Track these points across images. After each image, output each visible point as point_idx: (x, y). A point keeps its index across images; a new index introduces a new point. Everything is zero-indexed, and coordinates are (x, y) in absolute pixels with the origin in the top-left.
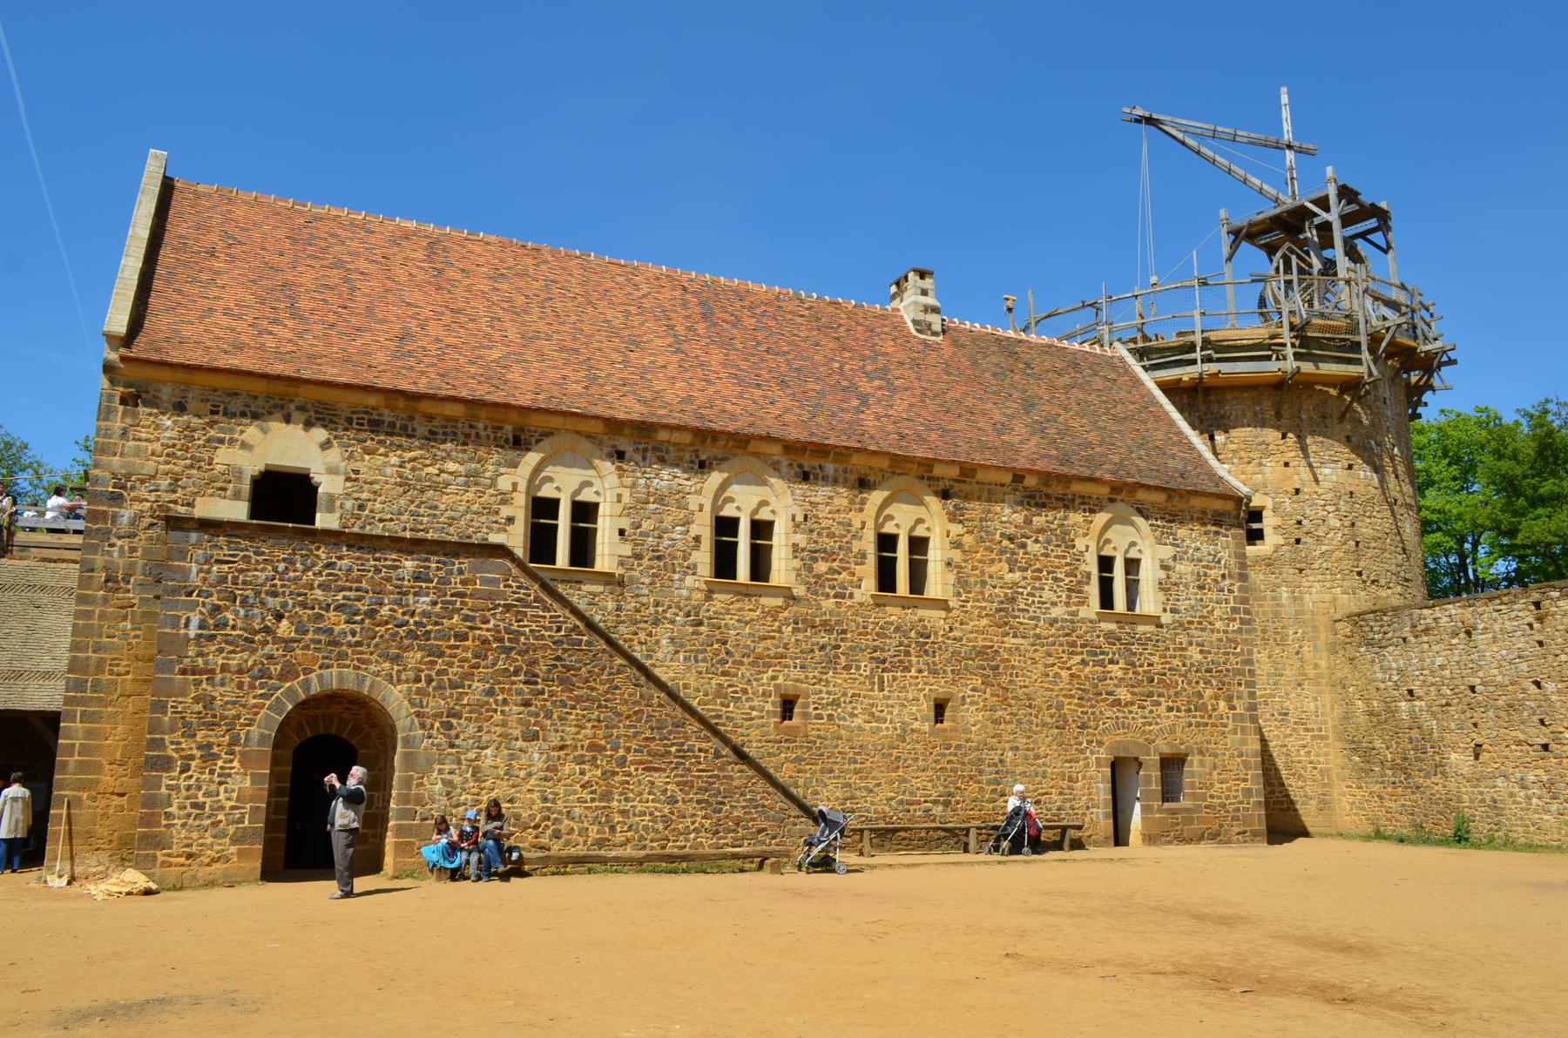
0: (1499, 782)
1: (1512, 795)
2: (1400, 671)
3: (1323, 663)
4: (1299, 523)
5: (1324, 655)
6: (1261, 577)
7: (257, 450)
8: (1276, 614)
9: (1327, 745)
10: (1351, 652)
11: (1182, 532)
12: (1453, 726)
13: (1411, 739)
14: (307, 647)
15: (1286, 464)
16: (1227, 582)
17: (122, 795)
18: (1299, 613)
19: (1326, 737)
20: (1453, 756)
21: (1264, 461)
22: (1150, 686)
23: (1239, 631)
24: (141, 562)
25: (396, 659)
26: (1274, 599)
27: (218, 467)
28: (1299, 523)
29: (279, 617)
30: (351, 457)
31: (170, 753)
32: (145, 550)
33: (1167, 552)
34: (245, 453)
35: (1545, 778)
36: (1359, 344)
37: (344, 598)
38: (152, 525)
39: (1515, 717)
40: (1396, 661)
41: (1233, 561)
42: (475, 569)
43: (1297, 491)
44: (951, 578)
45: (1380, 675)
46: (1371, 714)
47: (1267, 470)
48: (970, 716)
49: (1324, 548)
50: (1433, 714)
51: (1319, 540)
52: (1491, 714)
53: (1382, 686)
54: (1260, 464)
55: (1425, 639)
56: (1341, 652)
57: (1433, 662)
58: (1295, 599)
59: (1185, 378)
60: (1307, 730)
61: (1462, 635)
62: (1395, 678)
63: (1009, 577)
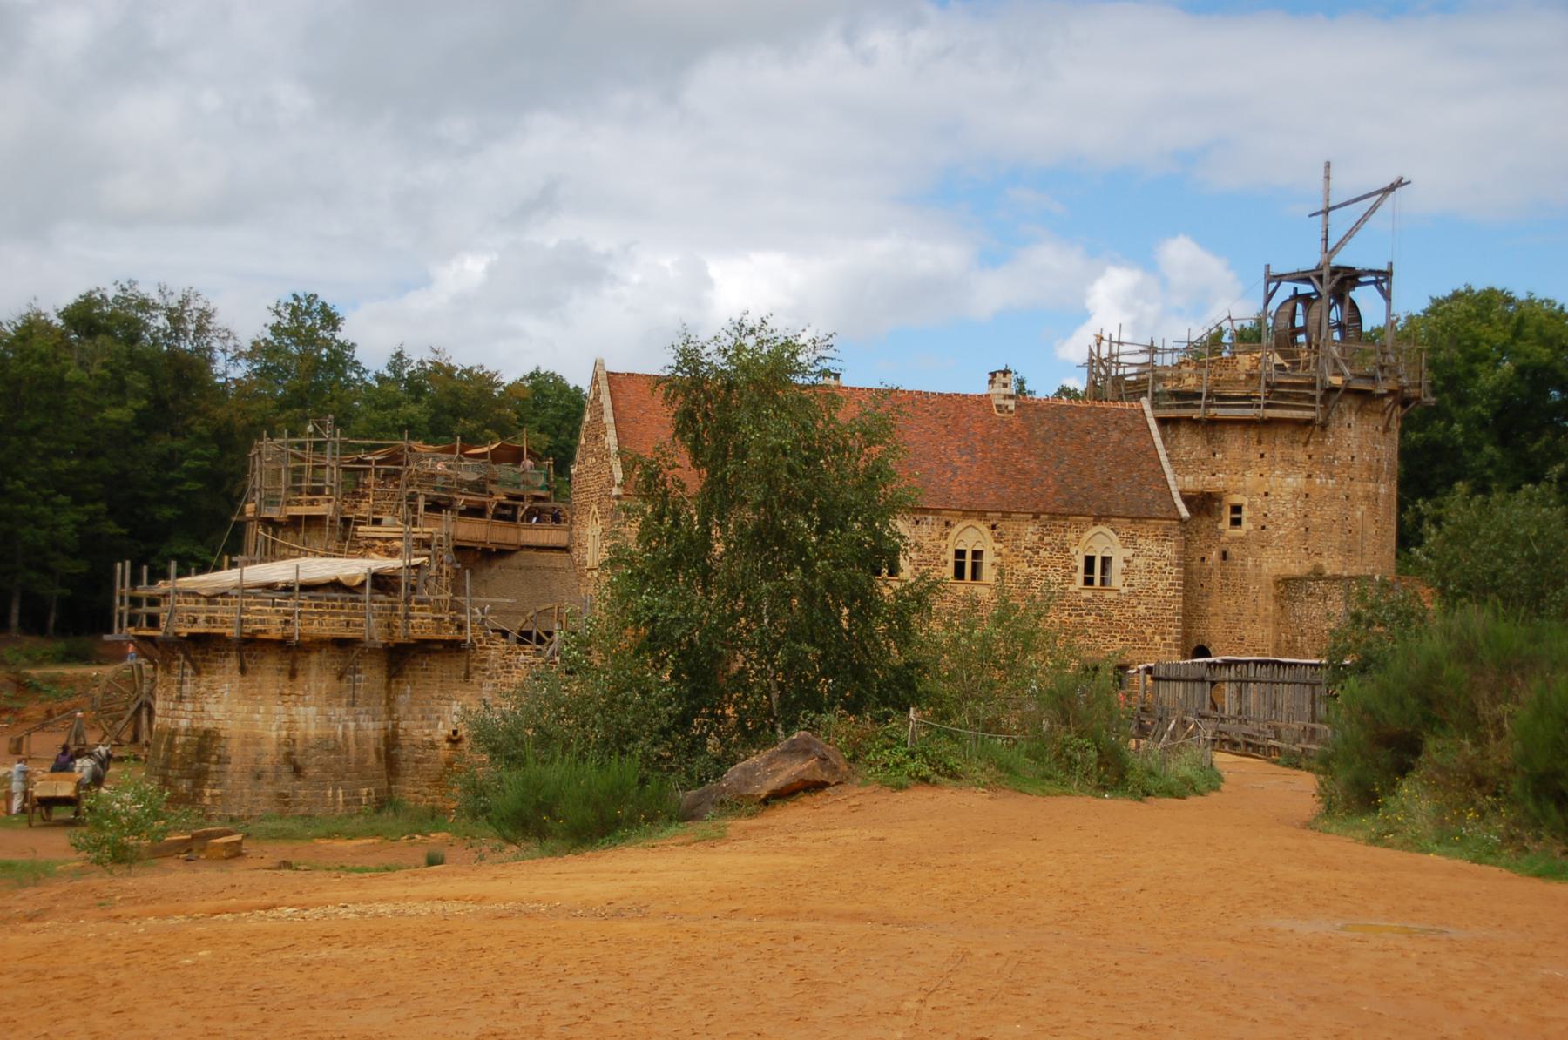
11: (1140, 541)
22: (1110, 627)
33: (1128, 553)
44: (995, 571)
51: (1278, 528)
63: (1028, 570)
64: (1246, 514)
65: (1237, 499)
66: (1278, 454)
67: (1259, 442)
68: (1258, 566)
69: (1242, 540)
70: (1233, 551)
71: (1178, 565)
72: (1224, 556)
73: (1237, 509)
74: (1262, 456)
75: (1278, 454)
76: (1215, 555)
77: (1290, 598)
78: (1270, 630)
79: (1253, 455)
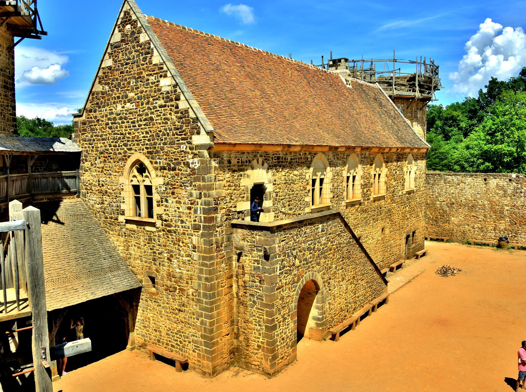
0: (466, 226)
1: (469, 230)
7: (251, 177)
13: (439, 213)
14: (302, 268)
17: (228, 335)
20: (453, 218)
24: (225, 236)
25: (318, 264)
27: (242, 188)
29: (295, 258)
30: (274, 174)
31: (276, 322)
32: (225, 230)
34: (247, 179)
35: (480, 226)
37: (309, 245)
38: (227, 219)
39: (474, 210)
42: (333, 223)
48: (387, 231)
52: (467, 208)
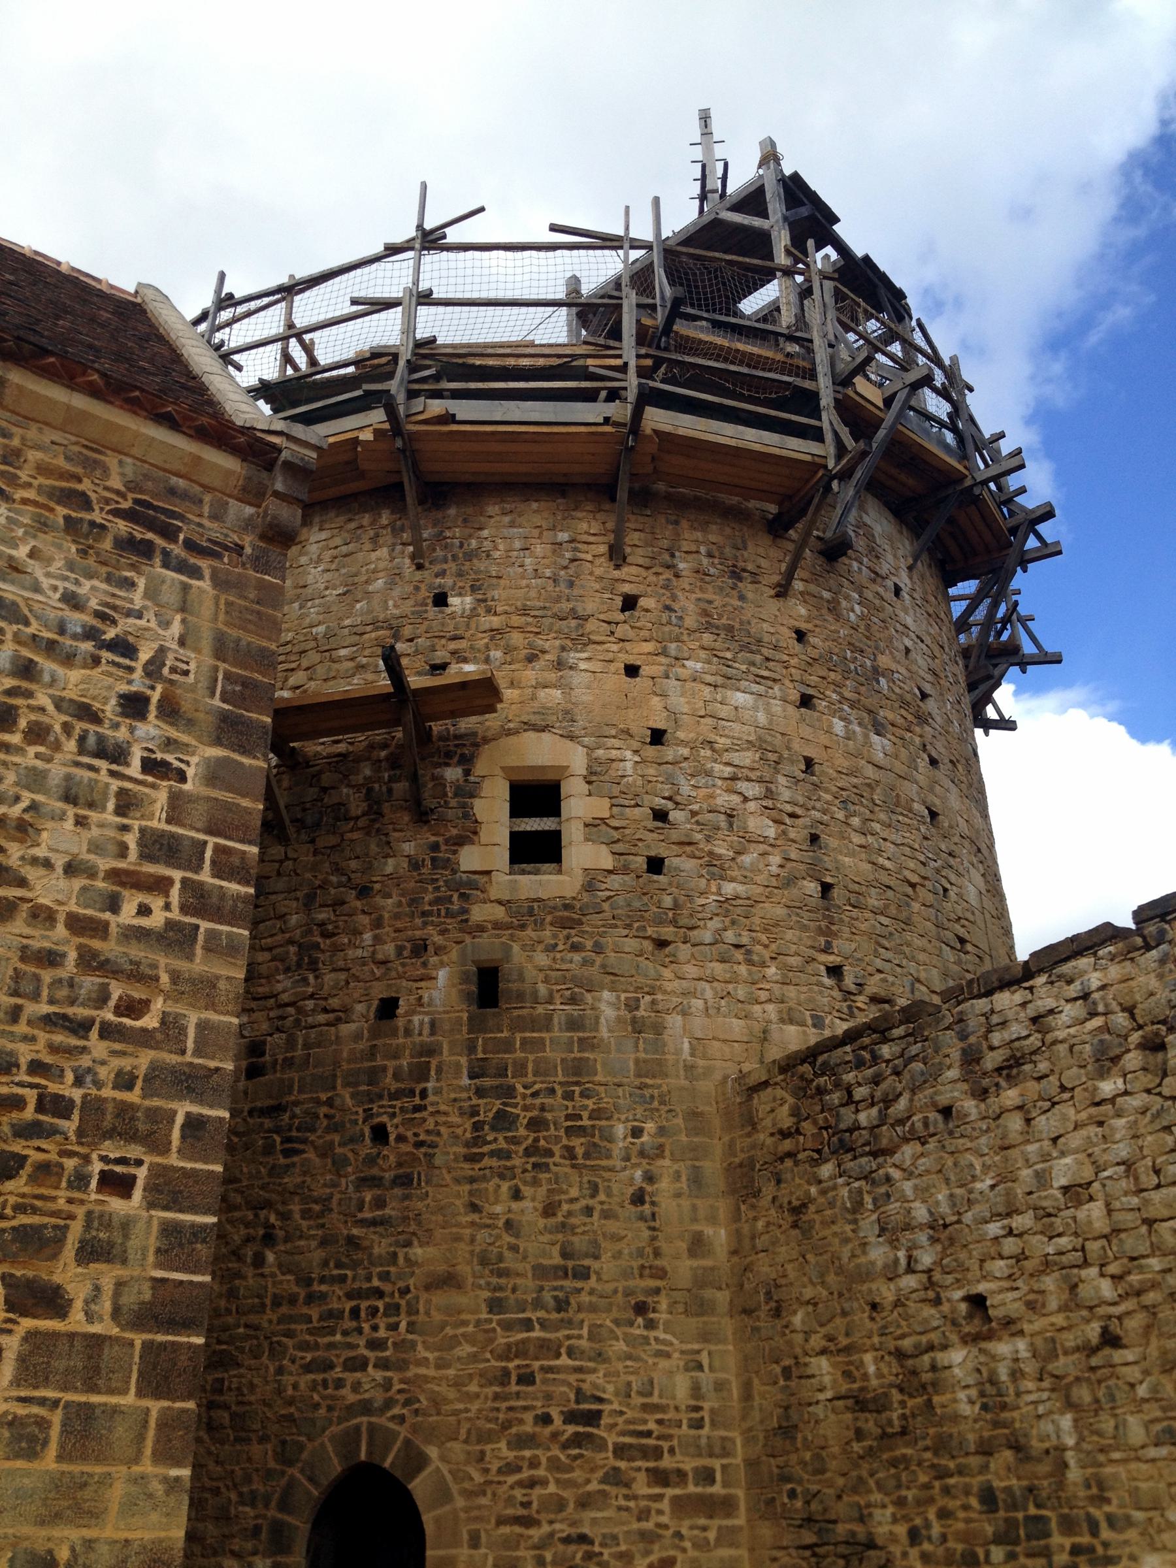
2: (937, 1226)
3: (719, 1236)
4: (660, 816)
5: (723, 1207)
6: (542, 959)
8: (578, 1068)
9: (727, 1537)
10: (797, 1186)
12: (1136, 1431)
13: (989, 1498)
15: (632, 671)
16: (151, 729)
18: (650, 1069)
19: (726, 1506)
21: (572, 657)
23: (177, 938)
26: (573, 1024)
28: (660, 816)
36: (814, 396)
40: (923, 1193)
41: (198, 662)
43: (658, 737)
45: (878, 1254)
46: (860, 1403)
47: (577, 679)
49: (729, 888)
50: (1061, 1387)
51: (715, 867)
53: (887, 1293)
54: (560, 665)
55: (1011, 1096)
56: (769, 1190)
57: (1042, 1179)
58: (638, 1027)
59: (367, 436)
60: (660, 1478)
61: (1133, 1060)
62: (926, 1259)
64: (579, 805)
65: (540, 752)
66: (688, 605)
67: (617, 555)
68: (642, 1027)
69: (566, 917)
70: (530, 962)
71: (228, 729)
72: (488, 987)
73: (537, 796)
74: (630, 603)
75: (688, 605)
76: (443, 987)
77: (842, 1144)
78: (725, 1360)
79: (596, 602)
